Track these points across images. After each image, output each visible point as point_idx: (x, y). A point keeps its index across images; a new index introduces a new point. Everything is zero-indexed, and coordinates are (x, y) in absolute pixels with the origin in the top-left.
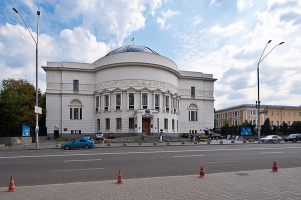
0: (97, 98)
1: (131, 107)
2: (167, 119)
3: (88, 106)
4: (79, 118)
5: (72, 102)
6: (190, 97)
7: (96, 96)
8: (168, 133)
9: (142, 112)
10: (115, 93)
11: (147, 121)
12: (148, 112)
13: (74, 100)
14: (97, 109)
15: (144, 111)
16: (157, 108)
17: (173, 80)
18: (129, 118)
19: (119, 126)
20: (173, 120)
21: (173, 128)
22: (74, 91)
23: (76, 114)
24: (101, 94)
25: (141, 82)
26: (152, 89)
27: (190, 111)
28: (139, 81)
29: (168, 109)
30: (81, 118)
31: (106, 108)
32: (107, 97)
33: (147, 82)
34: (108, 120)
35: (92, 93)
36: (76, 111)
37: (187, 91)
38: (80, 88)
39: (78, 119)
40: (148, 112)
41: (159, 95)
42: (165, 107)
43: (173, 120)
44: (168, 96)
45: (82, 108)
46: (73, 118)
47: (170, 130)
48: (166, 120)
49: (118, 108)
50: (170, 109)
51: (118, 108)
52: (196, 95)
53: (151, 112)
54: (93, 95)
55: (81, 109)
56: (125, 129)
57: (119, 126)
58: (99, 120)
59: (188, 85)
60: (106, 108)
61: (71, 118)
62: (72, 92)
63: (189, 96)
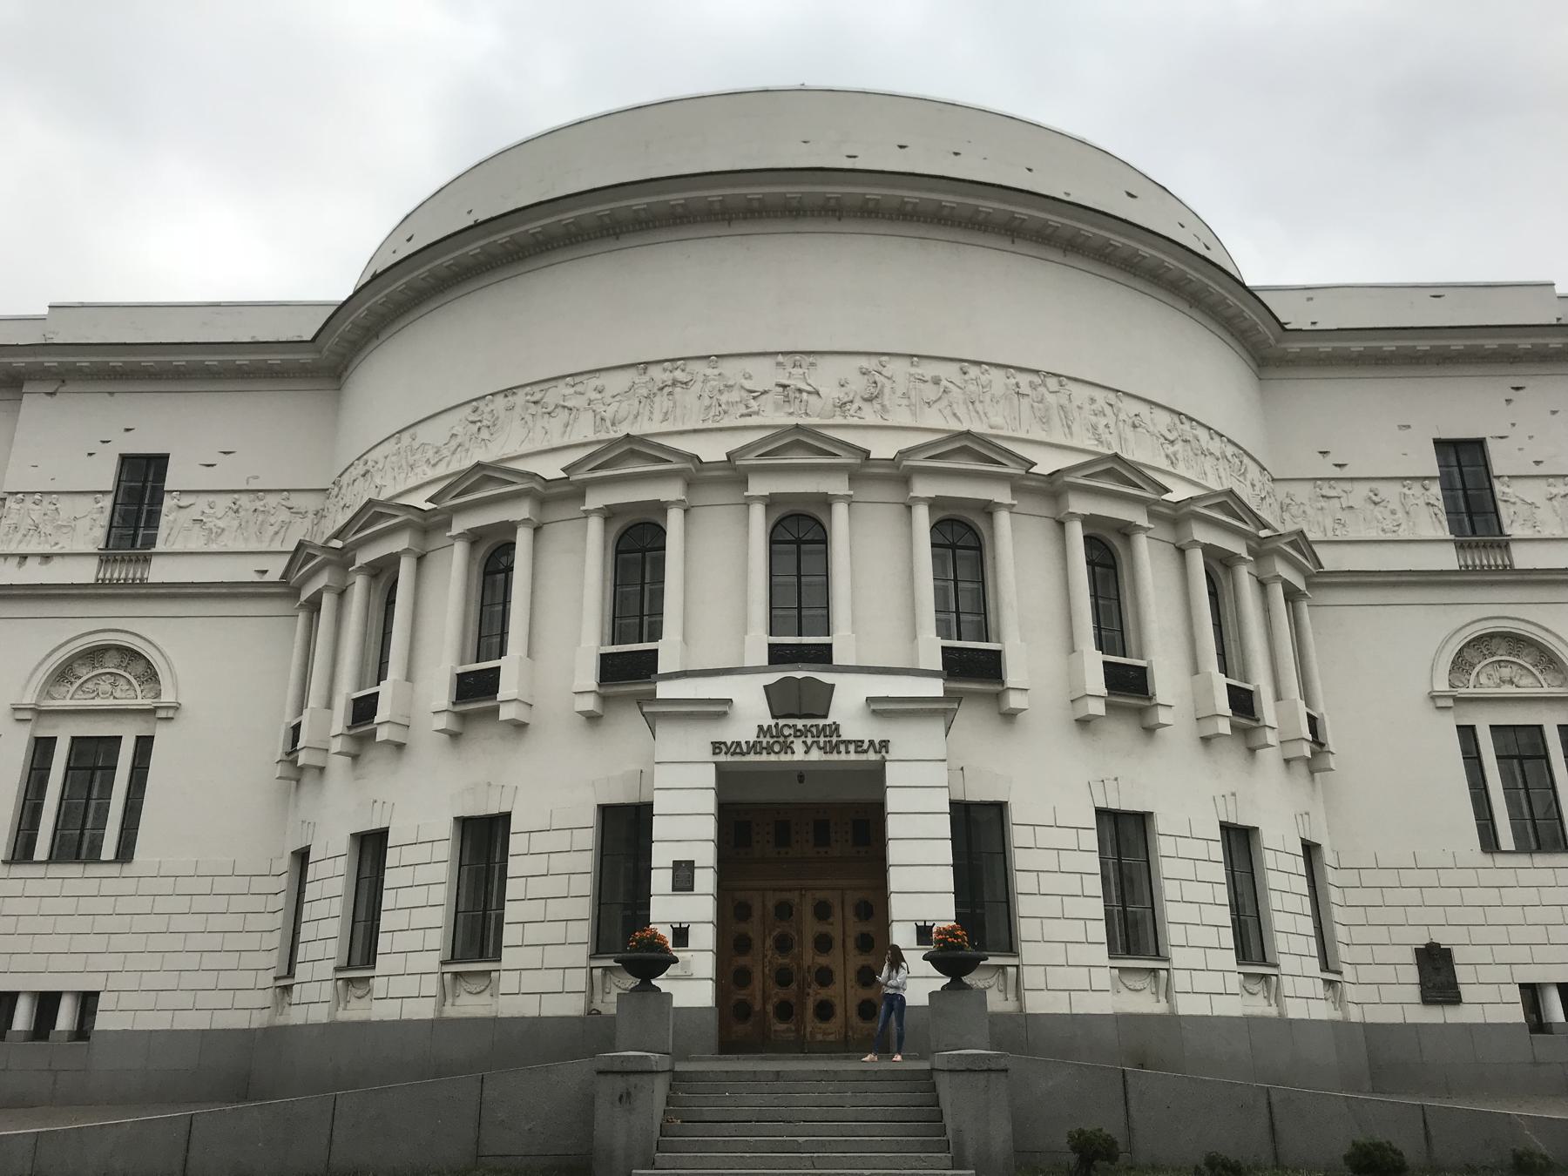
0: (314, 606)
1: (627, 672)
2: (1142, 820)
3: (221, 690)
4: (109, 849)
5: (63, 674)
6: (1447, 559)
7: (306, 594)
8: (1171, 1021)
9: (718, 710)
10: (461, 524)
11: (801, 839)
12: (799, 703)
13: (94, 655)
14: (296, 729)
15: (750, 708)
16: (974, 669)
17: (1197, 374)
18: (606, 811)
19: (477, 931)
20: (1239, 842)
21: (1250, 938)
22: (105, 558)
23: (85, 798)
24: (342, 560)
25: (764, 375)
26: (883, 448)
27: (1483, 722)
28: (730, 369)
29: (1128, 683)
30: (125, 852)
31: (364, 709)
32: (383, 574)
33: (828, 378)
34: (371, 847)
35: (275, 569)
36: (93, 757)
37: (1390, 492)
38: (175, 526)
39: (94, 857)
40: (799, 703)
41: (988, 509)
42: (1093, 664)
43: (1239, 842)
44: (1126, 531)
45: (164, 738)
46: (42, 849)
47: (1202, 976)
48: (1125, 837)
49: (476, 688)
50: (1168, 681)
51: (476, 688)
52: (1513, 529)
53: (849, 701)
54: (287, 589)
55: (144, 745)
56: (547, 964)
57: (477, 931)
58: (302, 857)
59: (1391, 433)
60: (364, 709)
61: (22, 852)
62: (86, 572)
63: (1423, 531)
